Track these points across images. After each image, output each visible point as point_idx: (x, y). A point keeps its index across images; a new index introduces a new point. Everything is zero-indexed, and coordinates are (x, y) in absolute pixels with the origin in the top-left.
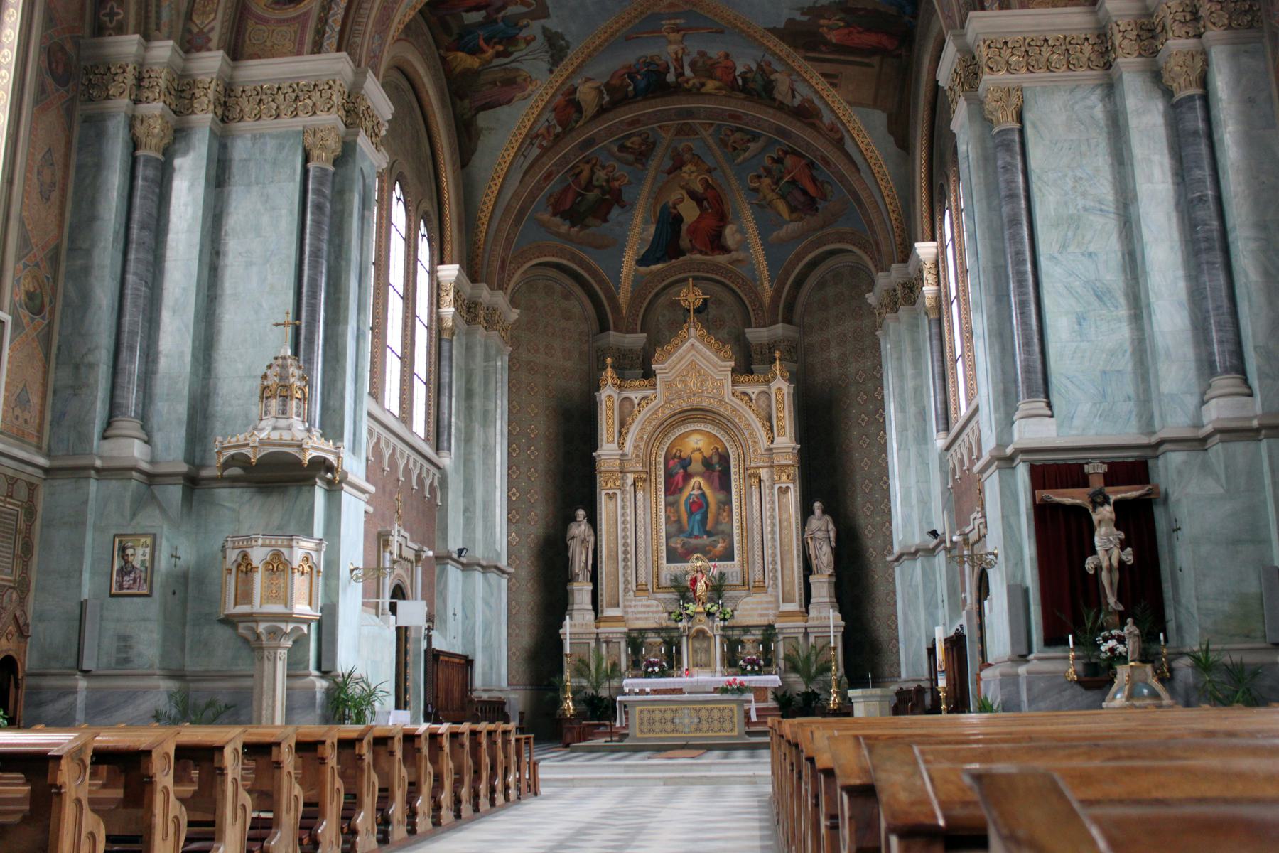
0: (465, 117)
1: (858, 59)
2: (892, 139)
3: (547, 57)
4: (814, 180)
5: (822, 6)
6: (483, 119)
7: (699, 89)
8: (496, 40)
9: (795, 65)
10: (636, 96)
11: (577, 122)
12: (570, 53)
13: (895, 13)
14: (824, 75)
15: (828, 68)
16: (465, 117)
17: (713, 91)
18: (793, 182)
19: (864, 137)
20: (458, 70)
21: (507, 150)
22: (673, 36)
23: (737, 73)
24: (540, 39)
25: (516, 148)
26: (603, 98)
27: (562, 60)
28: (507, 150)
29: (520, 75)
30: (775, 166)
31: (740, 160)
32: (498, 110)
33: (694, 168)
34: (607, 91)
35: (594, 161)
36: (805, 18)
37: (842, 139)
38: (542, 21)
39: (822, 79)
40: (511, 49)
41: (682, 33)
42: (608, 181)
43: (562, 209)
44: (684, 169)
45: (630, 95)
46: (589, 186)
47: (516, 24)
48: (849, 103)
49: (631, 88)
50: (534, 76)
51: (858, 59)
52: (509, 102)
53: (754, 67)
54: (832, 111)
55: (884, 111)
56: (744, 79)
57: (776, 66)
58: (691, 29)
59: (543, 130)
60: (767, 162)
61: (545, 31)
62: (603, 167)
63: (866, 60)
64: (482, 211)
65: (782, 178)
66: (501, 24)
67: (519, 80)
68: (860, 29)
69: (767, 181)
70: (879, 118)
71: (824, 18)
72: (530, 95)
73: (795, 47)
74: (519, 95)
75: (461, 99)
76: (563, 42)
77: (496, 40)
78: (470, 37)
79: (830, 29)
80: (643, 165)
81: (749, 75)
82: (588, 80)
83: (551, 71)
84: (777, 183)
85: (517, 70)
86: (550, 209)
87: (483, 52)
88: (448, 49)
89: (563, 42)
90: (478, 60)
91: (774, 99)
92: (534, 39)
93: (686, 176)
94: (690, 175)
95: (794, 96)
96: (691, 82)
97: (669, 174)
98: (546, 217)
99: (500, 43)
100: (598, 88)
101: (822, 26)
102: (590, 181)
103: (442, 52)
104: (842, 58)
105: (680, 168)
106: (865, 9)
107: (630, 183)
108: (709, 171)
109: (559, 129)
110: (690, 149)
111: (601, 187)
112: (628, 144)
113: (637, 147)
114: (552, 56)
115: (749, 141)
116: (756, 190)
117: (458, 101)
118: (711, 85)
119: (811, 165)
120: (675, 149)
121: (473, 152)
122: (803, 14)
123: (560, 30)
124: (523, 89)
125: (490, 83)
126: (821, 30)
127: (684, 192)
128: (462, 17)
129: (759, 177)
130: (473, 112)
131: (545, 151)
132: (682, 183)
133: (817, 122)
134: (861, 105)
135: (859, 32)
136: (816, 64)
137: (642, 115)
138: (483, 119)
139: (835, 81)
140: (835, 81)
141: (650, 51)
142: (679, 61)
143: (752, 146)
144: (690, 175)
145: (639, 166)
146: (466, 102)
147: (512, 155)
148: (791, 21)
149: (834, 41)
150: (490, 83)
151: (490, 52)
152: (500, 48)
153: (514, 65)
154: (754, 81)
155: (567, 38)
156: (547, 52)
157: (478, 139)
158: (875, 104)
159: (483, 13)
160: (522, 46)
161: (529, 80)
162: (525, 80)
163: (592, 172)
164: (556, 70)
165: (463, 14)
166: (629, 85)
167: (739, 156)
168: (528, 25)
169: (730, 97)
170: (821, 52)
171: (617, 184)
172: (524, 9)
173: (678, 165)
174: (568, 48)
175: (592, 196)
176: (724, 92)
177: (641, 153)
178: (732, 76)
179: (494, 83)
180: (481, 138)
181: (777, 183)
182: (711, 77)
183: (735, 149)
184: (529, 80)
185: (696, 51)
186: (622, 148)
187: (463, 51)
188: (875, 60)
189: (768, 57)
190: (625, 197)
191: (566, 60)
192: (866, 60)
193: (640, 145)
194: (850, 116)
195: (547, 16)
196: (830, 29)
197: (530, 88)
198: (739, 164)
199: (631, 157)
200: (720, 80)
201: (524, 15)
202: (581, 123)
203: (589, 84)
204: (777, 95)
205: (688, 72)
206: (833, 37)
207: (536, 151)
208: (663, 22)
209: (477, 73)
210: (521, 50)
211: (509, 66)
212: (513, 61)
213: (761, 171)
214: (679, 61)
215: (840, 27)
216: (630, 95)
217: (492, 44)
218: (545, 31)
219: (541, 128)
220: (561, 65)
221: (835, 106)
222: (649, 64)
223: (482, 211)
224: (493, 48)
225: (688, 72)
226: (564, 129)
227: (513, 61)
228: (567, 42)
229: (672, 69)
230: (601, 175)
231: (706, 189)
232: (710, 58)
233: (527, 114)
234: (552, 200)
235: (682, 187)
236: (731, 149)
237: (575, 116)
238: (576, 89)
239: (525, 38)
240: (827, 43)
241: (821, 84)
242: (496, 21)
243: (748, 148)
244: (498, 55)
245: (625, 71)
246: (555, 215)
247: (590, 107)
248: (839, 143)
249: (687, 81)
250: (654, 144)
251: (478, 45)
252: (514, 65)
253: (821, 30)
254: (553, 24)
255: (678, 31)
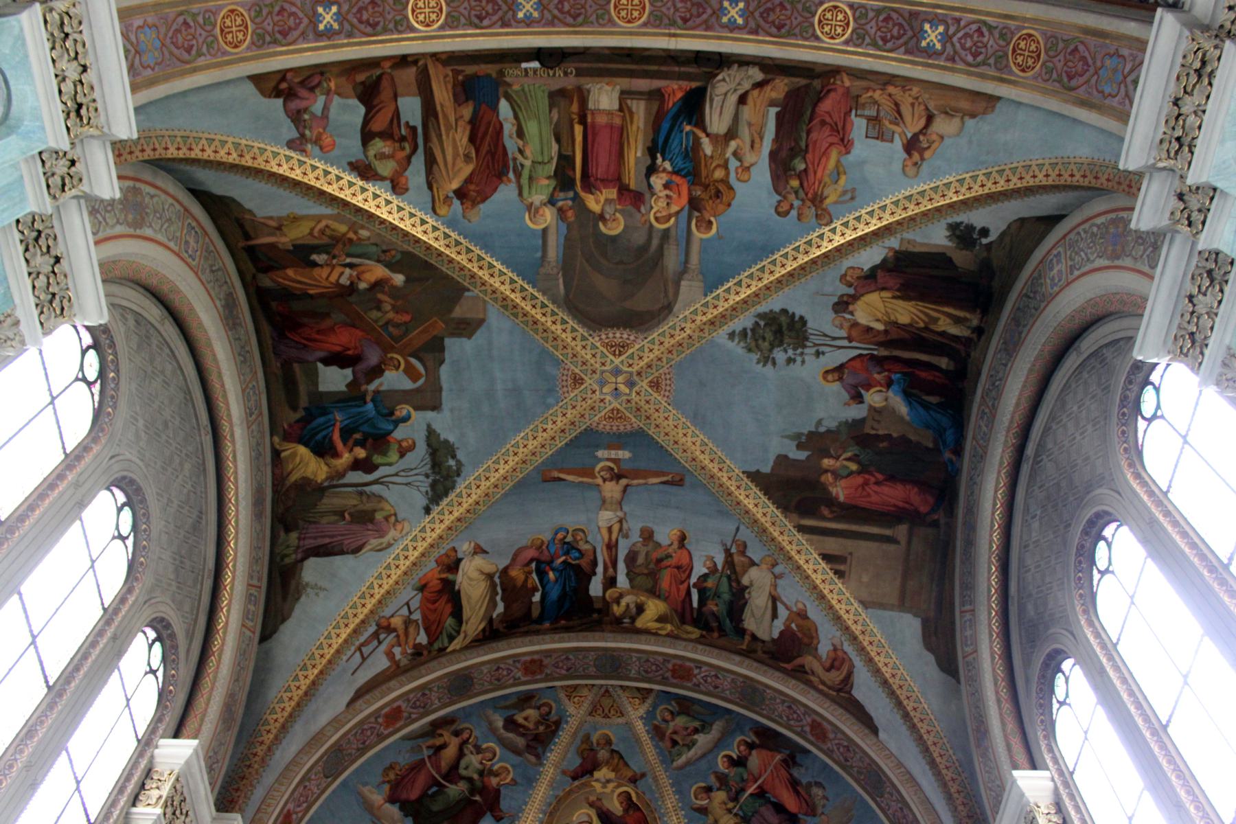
0: (287, 561)
1: (875, 530)
2: (930, 658)
3: (425, 484)
4: (794, 784)
5: (829, 431)
6: (312, 570)
7: (633, 619)
8: (357, 436)
9: (783, 540)
10: (540, 620)
11: (451, 638)
12: (461, 486)
13: (931, 445)
14: (827, 558)
15: (833, 545)
16: (287, 561)
17: (653, 625)
18: (761, 794)
19: (888, 656)
20: (294, 477)
21: (337, 627)
22: (612, 490)
23: (693, 580)
24: (422, 449)
25: (352, 626)
26: (495, 605)
27: (446, 495)
28: (337, 627)
29: (382, 509)
30: (733, 772)
31: (683, 759)
32: (338, 560)
33: (612, 775)
34: (503, 590)
35: (465, 735)
36: (802, 455)
37: (848, 680)
38: (430, 415)
39: (823, 564)
40: (377, 459)
41: (624, 482)
42: (481, 773)
43: (404, 796)
44: (597, 774)
45: (536, 612)
46: (452, 773)
47: (392, 414)
48: (865, 604)
49: (537, 597)
50: (400, 517)
51: (875, 530)
52: (356, 551)
53: (720, 559)
54: (838, 618)
55: (915, 615)
56: (702, 592)
57: (755, 553)
58: (636, 474)
59: (397, 622)
60: (721, 766)
61: (431, 433)
62: (478, 749)
63: (888, 532)
64: (273, 711)
65: (743, 790)
66: (370, 406)
67: (379, 516)
68: (880, 477)
69: (720, 796)
70: (909, 626)
71: (830, 456)
72: (389, 545)
73: (785, 507)
74: (374, 542)
75: (288, 530)
76: (452, 462)
77: (357, 436)
78: (322, 420)
79: (837, 475)
80: (538, 757)
81: (710, 583)
82: (479, 550)
83: (427, 510)
84: (735, 799)
85: (380, 498)
86: (387, 787)
87: (336, 455)
88: (287, 437)
89: (452, 462)
90: (325, 468)
91: (741, 632)
92: (412, 447)
93: (597, 786)
94: (604, 786)
95: (775, 615)
96: (624, 602)
97: (574, 778)
98: (377, 798)
99: (361, 443)
100: (490, 576)
101: (826, 471)
102: (455, 766)
103: (276, 439)
104: (854, 528)
105: (591, 773)
106: (888, 437)
107: (514, 782)
108: (634, 780)
109: (423, 638)
110: (609, 742)
111: (470, 780)
112: (519, 718)
113: (531, 726)
114: (433, 485)
115: (696, 731)
116: (703, 811)
117: (282, 534)
118: (654, 608)
119: (793, 756)
120: (587, 738)
121: (284, 620)
122: (800, 446)
123: (451, 439)
124: (381, 533)
125: (335, 513)
126: (823, 478)
127: (593, 813)
128: (316, 369)
129: (708, 790)
130: (300, 556)
131: (396, 672)
132: (592, 798)
133: (808, 661)
134: (882, 606)
135: (877, 483)
136: (815, 537)
137: (548, 653)
138: (312, 570)
139: (842, 568)
140: (842, 568)
141: (571, 520)
142: (612, 547)
143: (703, 740)
144: (604, 786)
145: (533, 759)
146: (294, 535)
147: (344, 636)
148: (782, 460)
149: (842, 498)
150: (335, 513)
151: (346, 458)
152: (361, 453)
153: (375, 488)
154: (717, 595)
155: (460, 455)
156: (427, 476)
157: (298, 599)
158: (903, 603)
159: (348, 372)
160: (393, 456)
161: (393, 519)
162: (387, 518)
163: (461, 754)
164: (436, 510)
165: (320, 365)
166: (535, 589)
167: (680, 755)
168: (406, 419)
169: (677, 637)
170: (824, 518)
171: (494, 781)
172: (408, 385)
173: (587, 768)
174: (459, 475)
175: (455, 790)
176: (669, 627)
177: (536, 738)
178: (685, 585)
179: (341, 514)
180: (303, 599)
181: (735, 799)
182: (654, 592)
183: (675, 743)
184: (393, 519)
185: (640, 525)
186: (510, 724)
187: (306, 445)
188: (901, 531)
189: (746, 534)
190: (504, 804)
191: (452, 496)
192: (888, 532)
193: (538, 723)
194: (865, 624)
195: (436, 407)
196: (837, 475)
197: (392, 534)
198: (682, 768)
199: (521, 742)
200: (666, 599)
201: (406, 397)
202: (456, 644)
203: (479, 561)
204: (749, 624)
205: (622, 581)
206: (840, 491)
207: (380, 663)
208: (601, 453)
209: (321, 490)
210: (390, 464)
211: (367, 489)
212: (376, 482)
213: (712, 780)
214: (612, 547)
215: (852, 473)
216: (536, 612)
217: (351, 443)
218: (431, 433)
219: (396, 614)
220: (445, 501)
221: (841, 608)
222: (569, 547)
223: (273, 711)
224: (351, 451)
225: (622, 581)
226: (431, 643)
227: (376, 482)
228: (459, 464)
229: (600, 569)
230: (473, 761)
231: (626, 810)
232: (658, 545)
233: (380, 577)
234: (392, 776)
235: (591, 805)
236: (668, 744)
237: (450, 622)
238: (459, 561)
239: (399, 442)
240: (831, 502)
241: (819, 572)
242: (362, 399)
243: (694, 743)
244: (357, 465)
245: (532, 553)
246: (392, 800)
247: (473, 624)
248: (844, 696)
249: (618, 601)
250: (558, 724)
251: (331, 440)
252: (375, 488)
253: (823, 478)
254: (443, 423)
255: (618, 477)
